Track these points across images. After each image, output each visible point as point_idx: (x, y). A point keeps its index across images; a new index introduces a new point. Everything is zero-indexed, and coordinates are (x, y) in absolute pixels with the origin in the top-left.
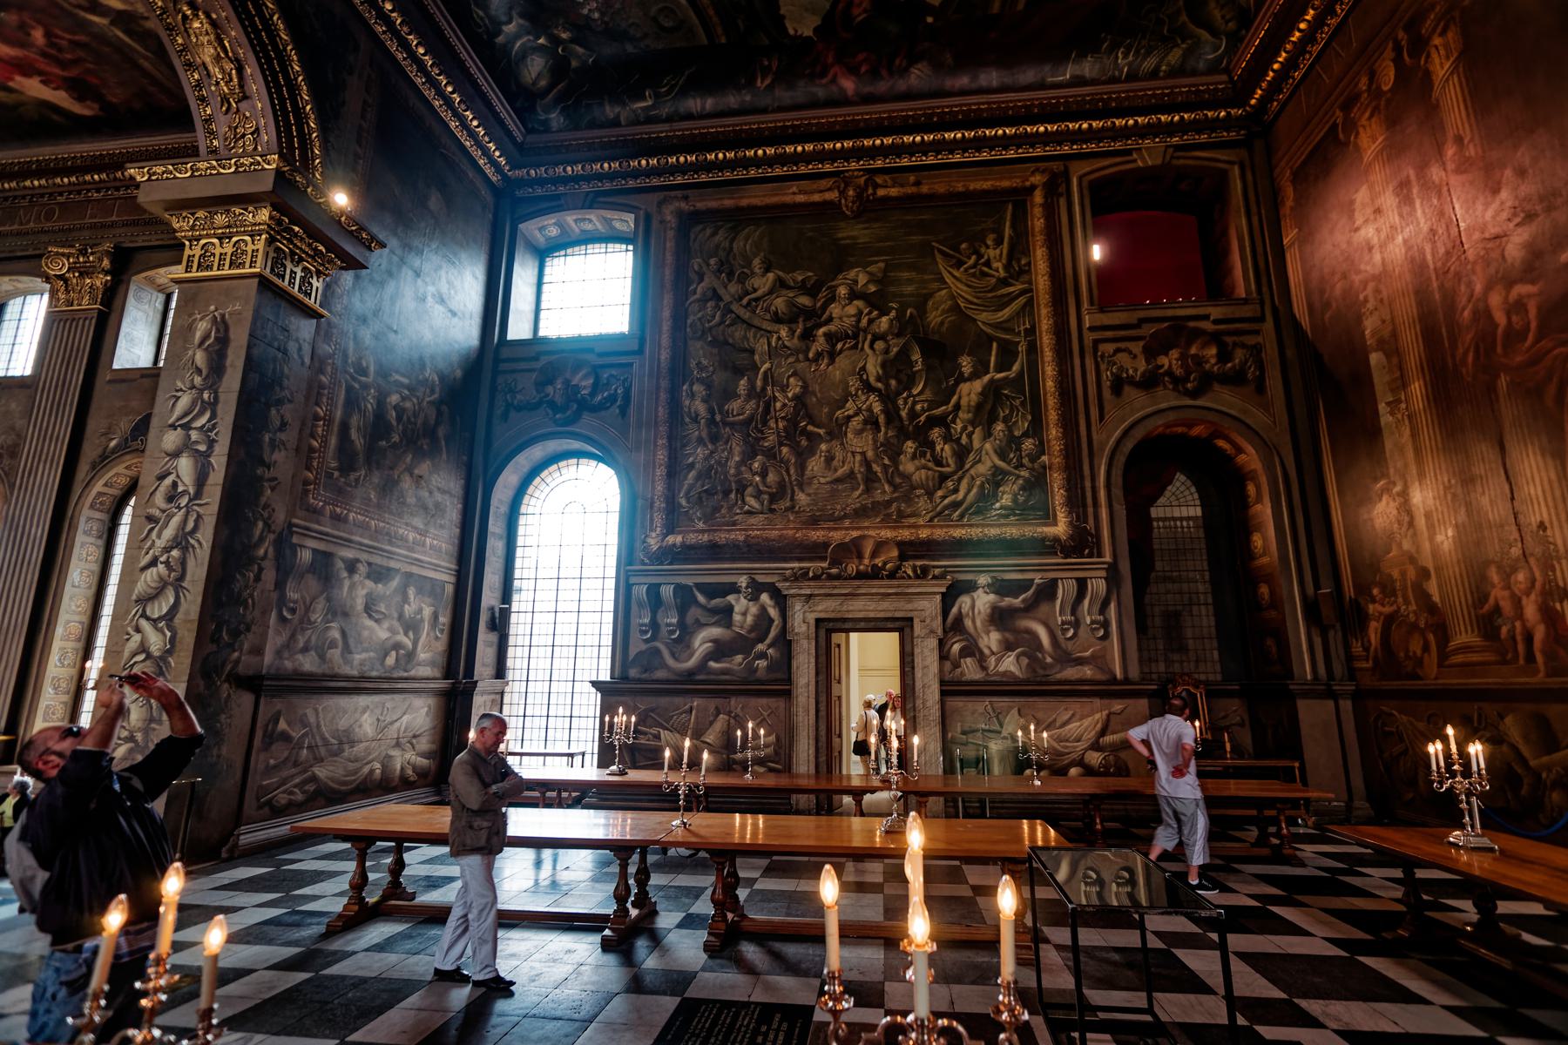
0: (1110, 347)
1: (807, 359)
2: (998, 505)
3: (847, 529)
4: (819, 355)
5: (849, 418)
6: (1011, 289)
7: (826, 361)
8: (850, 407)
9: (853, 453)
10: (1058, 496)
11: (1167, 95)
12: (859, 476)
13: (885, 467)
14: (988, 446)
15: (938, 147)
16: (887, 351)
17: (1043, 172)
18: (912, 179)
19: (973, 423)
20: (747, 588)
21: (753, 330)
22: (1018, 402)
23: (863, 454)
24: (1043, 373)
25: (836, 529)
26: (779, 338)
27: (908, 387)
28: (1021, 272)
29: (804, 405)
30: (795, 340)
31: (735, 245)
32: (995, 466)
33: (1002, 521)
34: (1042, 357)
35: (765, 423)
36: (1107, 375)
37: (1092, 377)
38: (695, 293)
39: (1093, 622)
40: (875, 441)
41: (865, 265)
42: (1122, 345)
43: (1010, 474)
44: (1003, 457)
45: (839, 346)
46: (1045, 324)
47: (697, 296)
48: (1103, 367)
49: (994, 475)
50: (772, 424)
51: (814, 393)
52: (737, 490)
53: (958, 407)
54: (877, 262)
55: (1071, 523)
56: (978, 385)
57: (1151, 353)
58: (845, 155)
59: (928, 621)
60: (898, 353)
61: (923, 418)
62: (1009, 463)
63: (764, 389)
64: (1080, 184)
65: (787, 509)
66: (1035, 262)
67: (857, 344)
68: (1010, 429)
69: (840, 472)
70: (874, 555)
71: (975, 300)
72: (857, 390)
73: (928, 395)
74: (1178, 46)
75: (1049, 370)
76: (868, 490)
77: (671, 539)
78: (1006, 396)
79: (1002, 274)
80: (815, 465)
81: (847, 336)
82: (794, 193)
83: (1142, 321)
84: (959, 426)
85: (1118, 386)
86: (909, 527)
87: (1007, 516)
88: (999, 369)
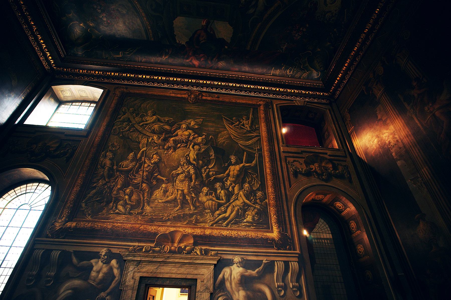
0: (291, 160)
1: (164, 149)
2: (245, 220)
3: (168, 226)
4: (169, 148)
5: (178, 174)
6: (252, 134)
7: (172, 150)
8: (180, 170)
9: (177, 190)
10: (273, 218)
11: (304, 84)
12: (179, 201)
13: (192, 198)
14: (241, 193)
15: (227, 88)
16: (199, 150)
17: (264, 101)
18: (216, 96)
19: (235, 182)
20: (104, 256)
21: (142, 135)
22: (255, 176)
23: (183, 191)
24: (265, 166)
25: (162, 226)
26: (153, 139)
27: (207, 165)
28: (256, 130)
29: (158, 167)
30: (160, 141)
31: (142, 105)
32: (244, 202)
33: (247, 229)
34: (265, 160)
35: (137, 172)
36: (291, 170)
37: (285, 170)
38: (120, 118)
39: (294, 287)
40: (189, 186)
41: (194, 119)
42: (297, 159)
43: (252, 206)
44: (247, 199)
45: (179, 145)
46: (265, 148)
47: (121, 120)
48: (289, 166)
49: (244, 206)
50: (141, 173)
51: (164, 162)
52: (114, 202)
53: (228, 175)
54: (199, 118)
55: (280, 232)
56: (237, 167)
57: (307, 163)
58: (193, 84)
59: (205, 282)
60: (204, 151)
61: (212, 178)
62: (250, 202)
63: (141, 158)
64: (276, 106)
65: (138, 214)
66: (261, 127)
67: (187, 145)
68: (251, 187)
69: (170, 198)
70: (181, 241)
71: (238, 136)
72: (184, 163)
73: (215, 169)
74: (306, 72)
75: (267, 164)
76: (182, 208)
77: (69, 224)
78: (250, 173)
79: (249, 129)
80: (158, 193)
81: (183, 142)
82: (170, 93)
83: (302, 152)
84: (229, 183)
85: (296, 174)
86: (200, 228)
87: (249, 226)
88: (247, 162)
